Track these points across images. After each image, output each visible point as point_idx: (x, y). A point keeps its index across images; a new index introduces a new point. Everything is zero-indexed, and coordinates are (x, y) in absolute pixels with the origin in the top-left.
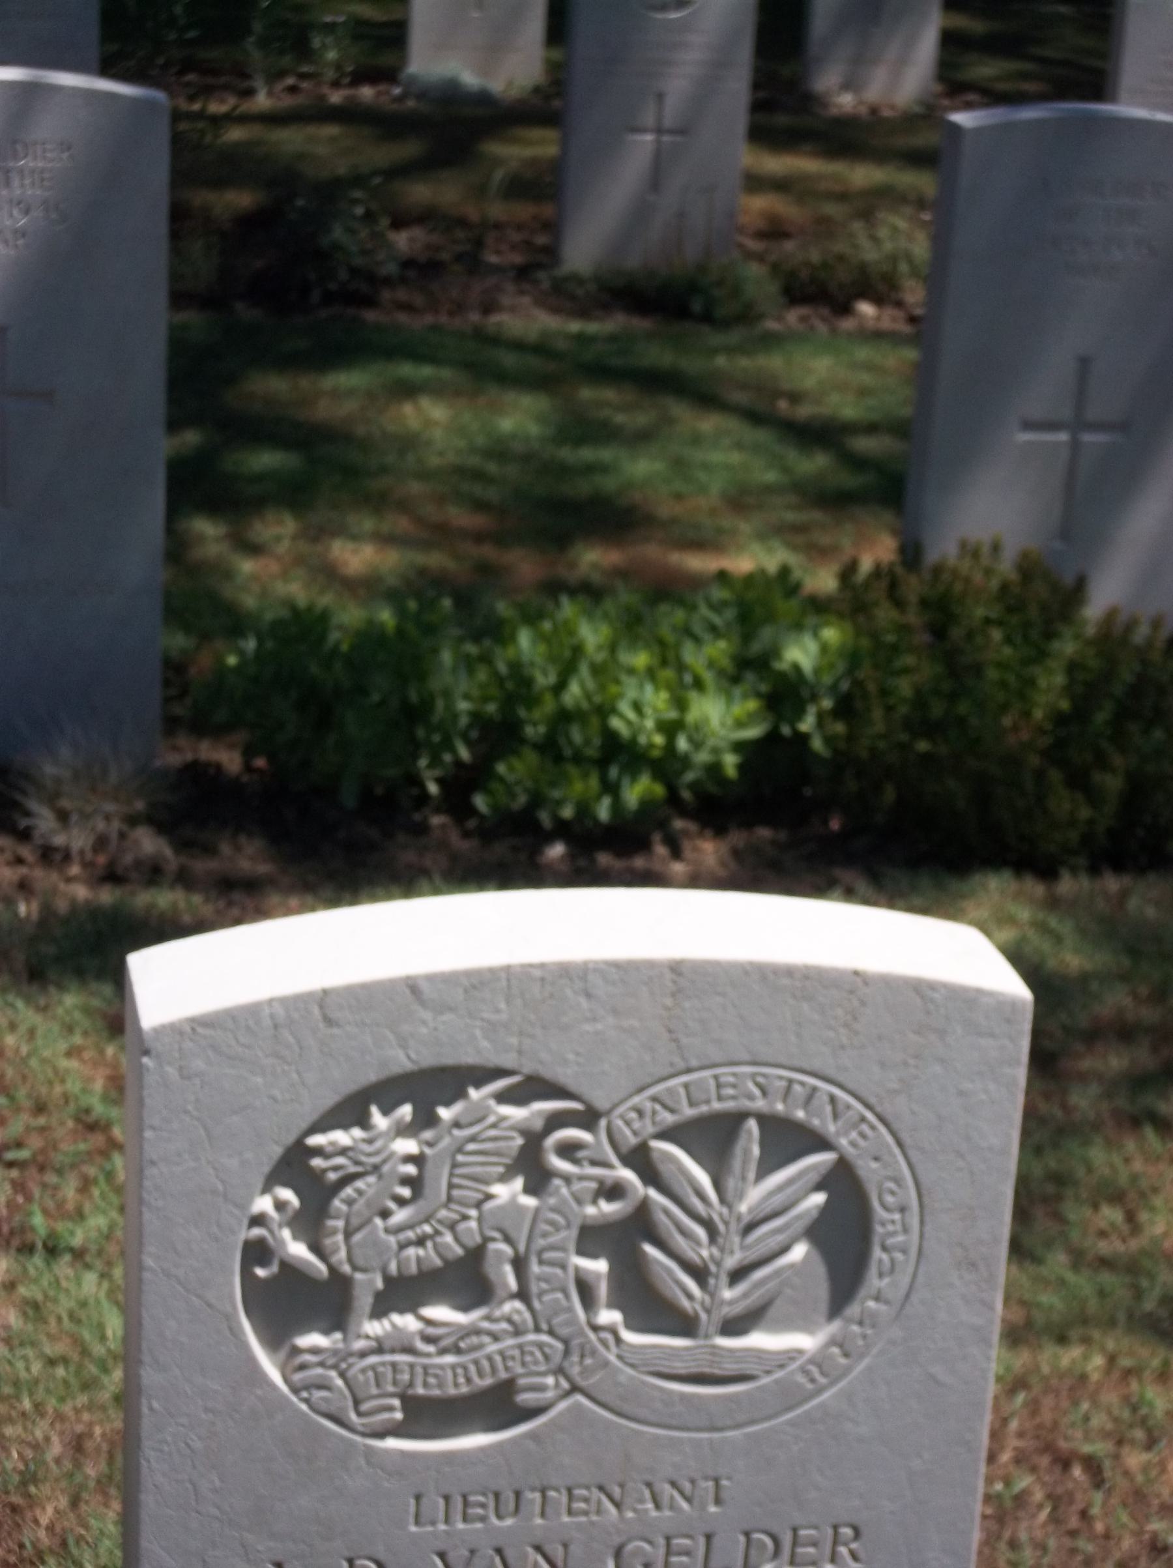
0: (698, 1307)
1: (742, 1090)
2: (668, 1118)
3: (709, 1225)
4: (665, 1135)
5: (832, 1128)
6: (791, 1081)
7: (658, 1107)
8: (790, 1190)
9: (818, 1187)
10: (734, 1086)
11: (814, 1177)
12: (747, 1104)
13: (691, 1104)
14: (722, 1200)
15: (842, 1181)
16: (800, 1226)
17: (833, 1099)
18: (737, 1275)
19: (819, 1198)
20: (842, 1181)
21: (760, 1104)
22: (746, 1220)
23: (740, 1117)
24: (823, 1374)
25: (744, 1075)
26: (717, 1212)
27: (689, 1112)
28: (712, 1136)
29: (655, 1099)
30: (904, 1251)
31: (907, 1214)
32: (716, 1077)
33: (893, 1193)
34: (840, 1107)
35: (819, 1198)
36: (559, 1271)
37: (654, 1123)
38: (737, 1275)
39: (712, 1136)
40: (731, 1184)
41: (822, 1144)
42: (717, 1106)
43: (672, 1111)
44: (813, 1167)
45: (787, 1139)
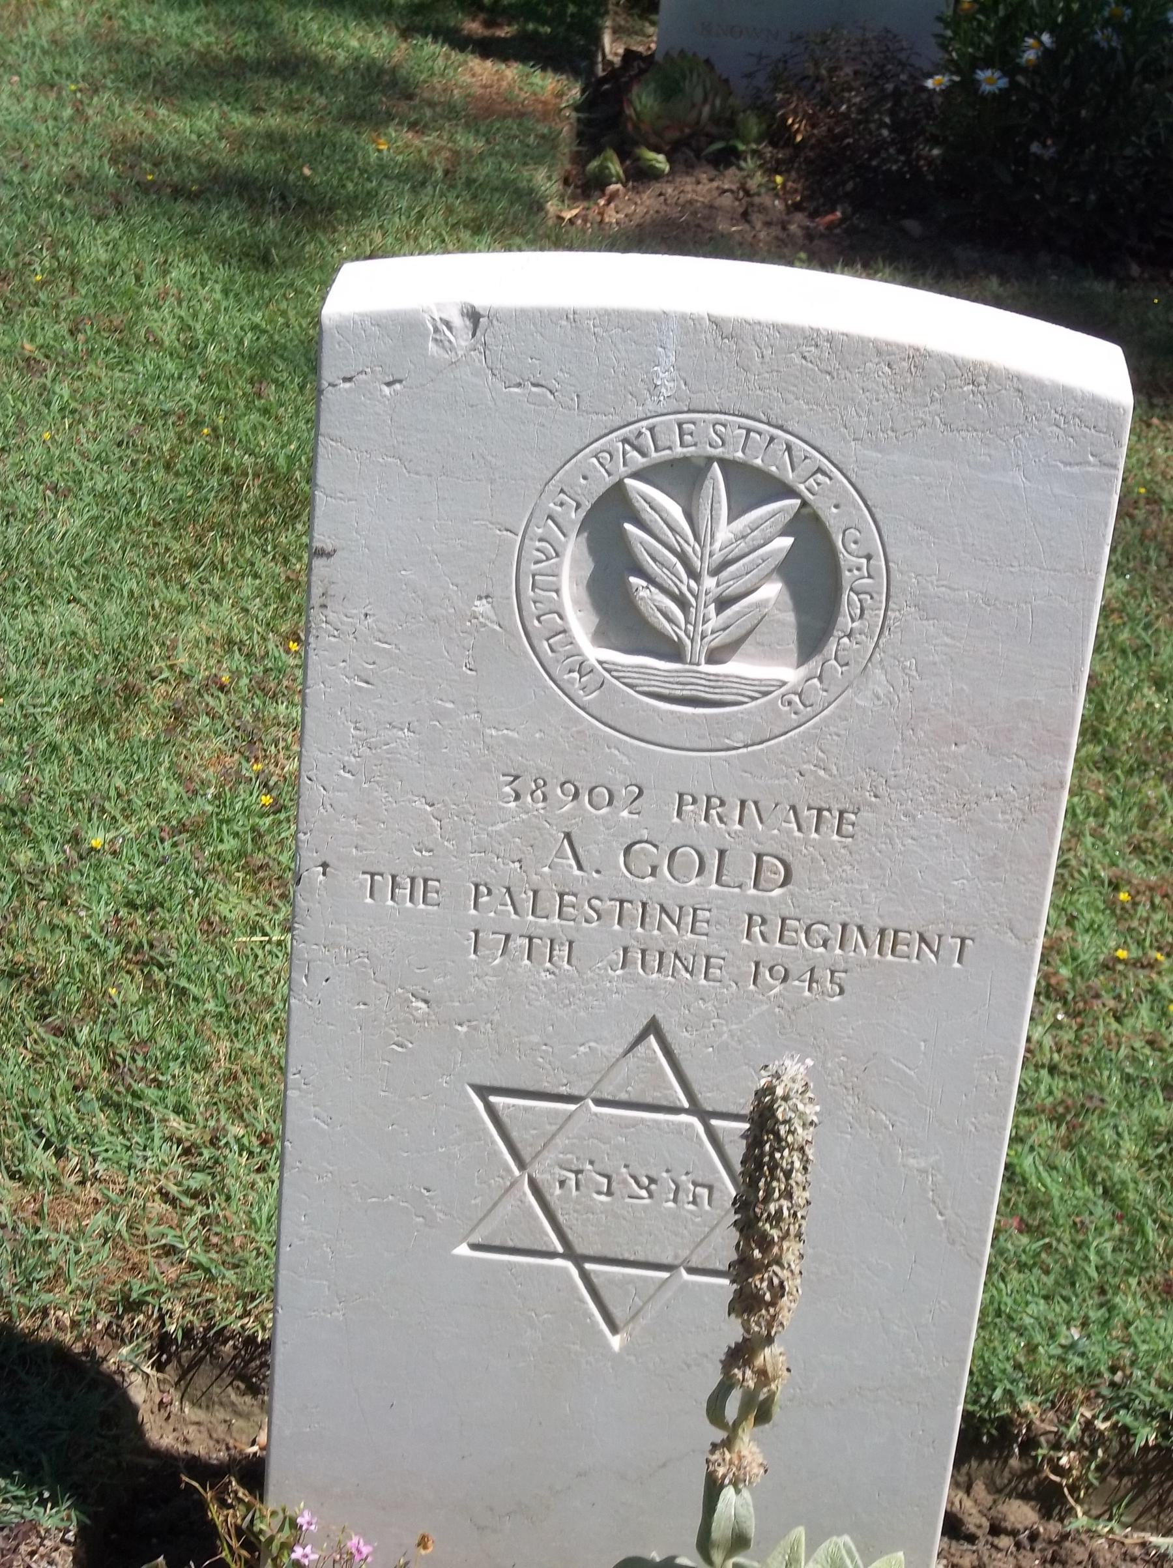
0: (682, 634)
1: (714, 437)
2: (639, 460)
4: (636, 475)
6: (749, 431)
7: (627, 447)
8: (766, 531)
9: (784, 533)
12: (711, 451)
13: (656, 450)
15: (808, 527)
16: (773, 563)
19: (788, 541)
20: (808, 527)
21: (718, 452)
23: (710, 460)
28: (683, 476)
29: (625, 441)
32: (680, 425)
35: (788, 541)
36: (554, 595)
37: (625, 464)
39: (683, 476)
40: (704, 524)
41: (791, 493)
42: (679, 451)
43: (643, 454)
45: (752, 486)
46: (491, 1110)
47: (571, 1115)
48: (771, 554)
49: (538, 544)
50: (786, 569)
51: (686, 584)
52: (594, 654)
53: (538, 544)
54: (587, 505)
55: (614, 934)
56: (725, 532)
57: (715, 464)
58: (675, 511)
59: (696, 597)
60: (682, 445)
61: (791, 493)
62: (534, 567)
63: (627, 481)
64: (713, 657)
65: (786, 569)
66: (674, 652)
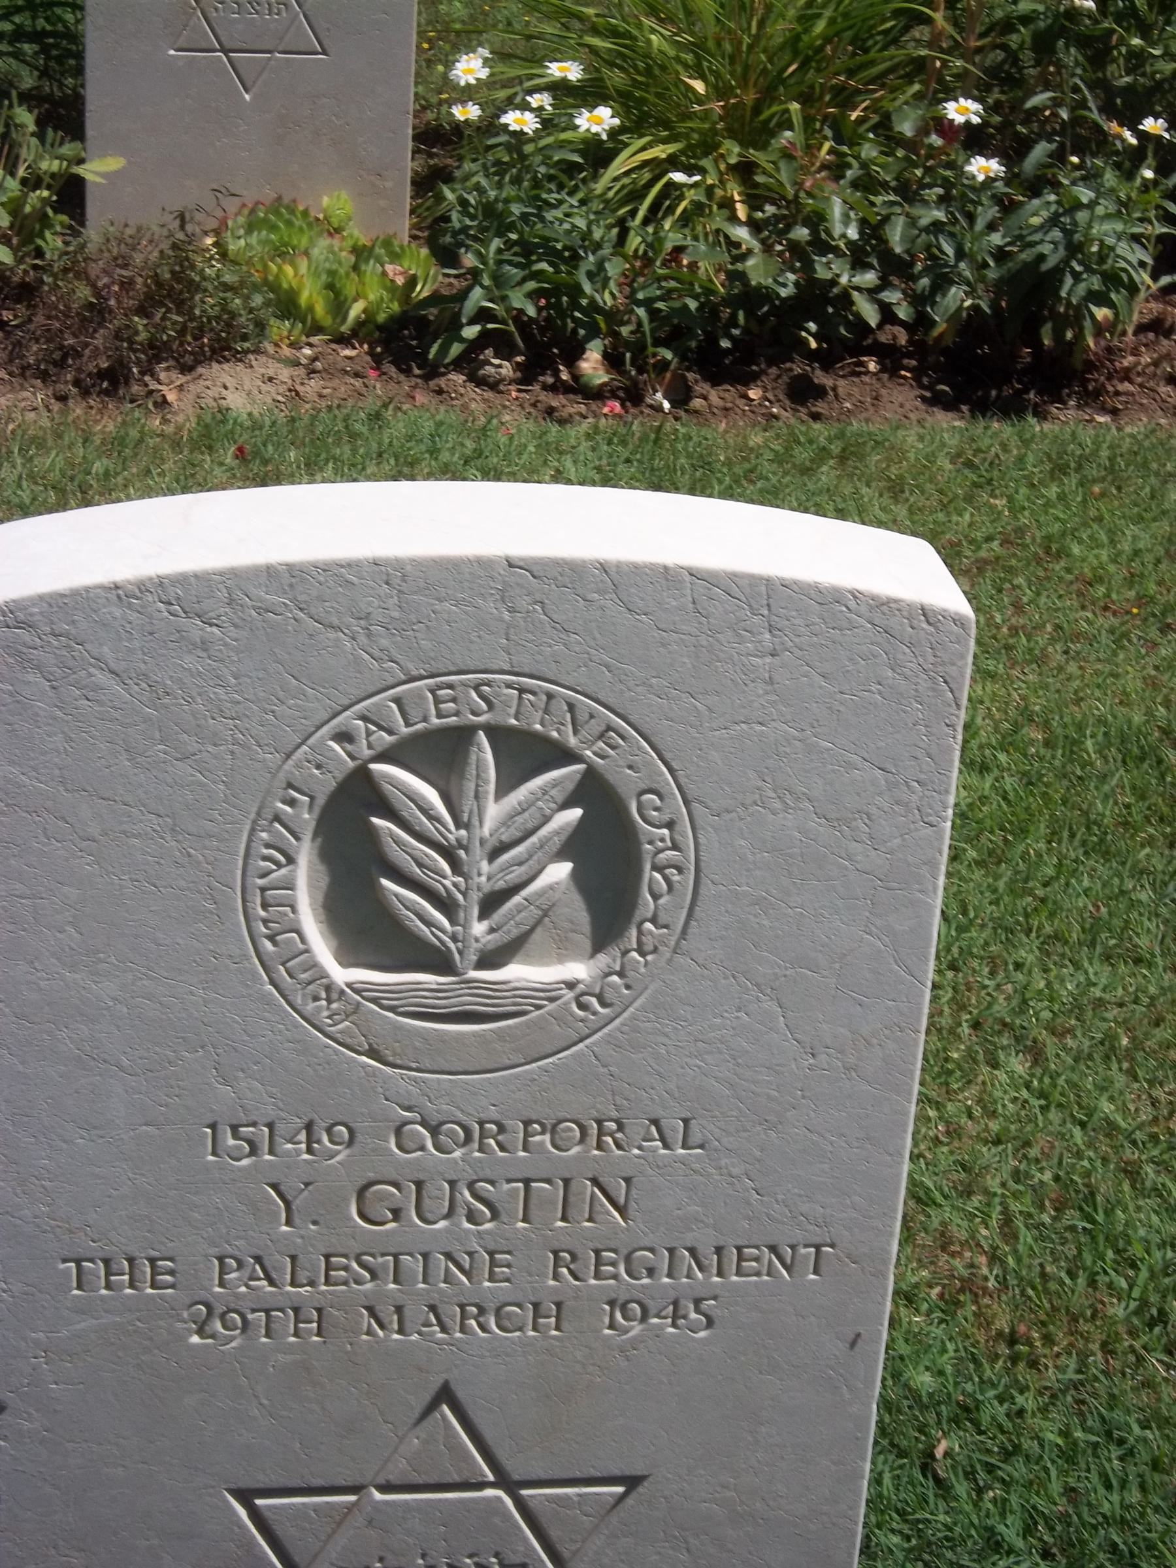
3: (447, 853)
5: (573, 741)
10: (454, 700)
11: (559, 795)
13: (408, 724)
14: (458, 825)
17: (571, 707)
18: (491, 903)
22: (492, 843)
23: (471, 730)
24: (603, 1004)
25: (464, 684)
26: (454, 834)
27: (405, 730)
28: (441, 753)
30: (680, 870)
31: (677, 828)
33: (656, 809)
34: (582, 716)
37: (370, 747)
38: (491, 903)
40: (468, 805)
41: (567, 756)
43: (390, 732)
44: (555, 784)
45: (525, 754)
46: (256, 1515)
47: (351, 1507)
48: (557, 833)
49: (266, 851)
50: (572, 846)
51: (450, 881)
52: (341, 975)
53: (266, 851)
54: (321, 800)
55: (419, 1293)
56: (494, 811)
57: (481, 733)
58: (431, 795)
59: (464, 894)
60: (440, 715)
61: (567, 756)
62: (260, 882)
63: (373, 766)
64: (491, 959)
65: (572, 846)
66: (441, 963)
